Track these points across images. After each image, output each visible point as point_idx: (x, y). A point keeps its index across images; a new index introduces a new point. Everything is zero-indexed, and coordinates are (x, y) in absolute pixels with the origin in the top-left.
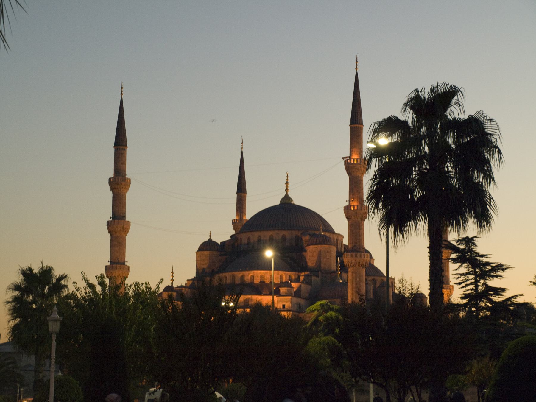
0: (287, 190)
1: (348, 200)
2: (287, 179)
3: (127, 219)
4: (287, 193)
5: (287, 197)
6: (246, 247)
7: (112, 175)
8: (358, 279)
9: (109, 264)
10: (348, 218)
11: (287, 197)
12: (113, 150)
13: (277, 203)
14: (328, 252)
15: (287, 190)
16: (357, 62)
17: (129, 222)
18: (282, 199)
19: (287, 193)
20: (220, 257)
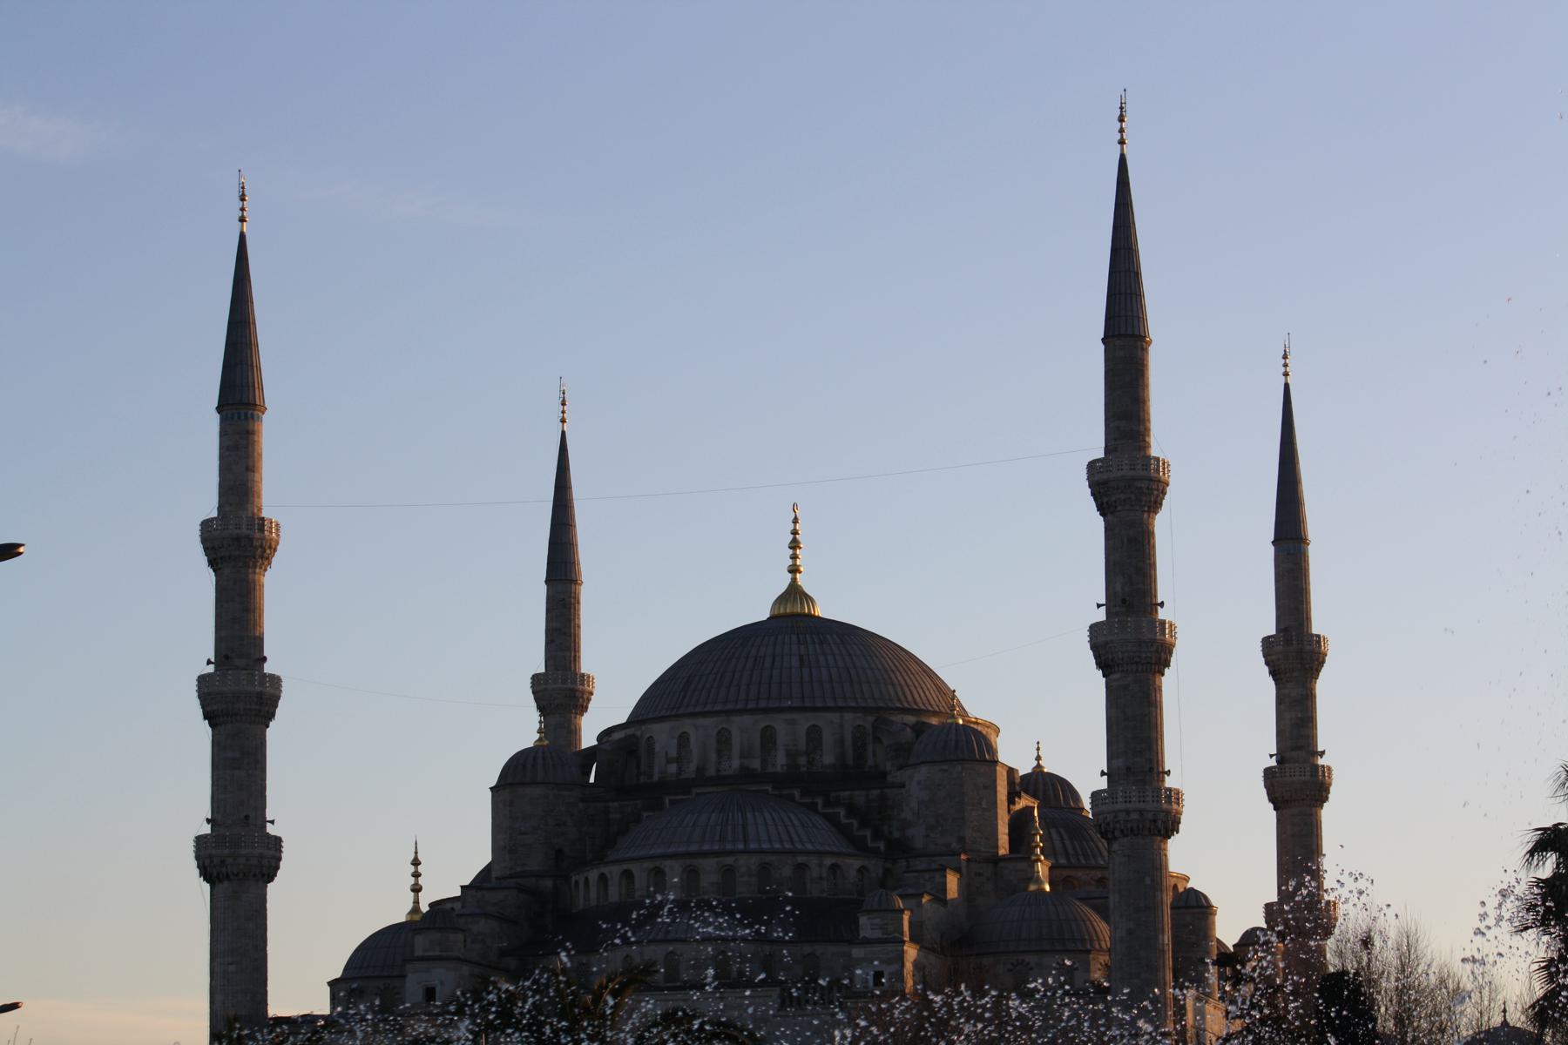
0: (794, 570)
1: (1103, 601)
2: (795, 532)
3: (268, 668)
4: (794, 580)
5: (794, 593)
6: (673, 768)
7: (210, 509)
8: (1148, 881)
9: (206, 829)
10: (1104, 664)
11: (794, 593)
12: (214, 420)
13: (762, 613)
14: (986, 788)
15: (794, 570)
16: (1121, 119)
17: (276, 681)
18: (782, 600)
19: (794, 580)
20: (581, 805)
